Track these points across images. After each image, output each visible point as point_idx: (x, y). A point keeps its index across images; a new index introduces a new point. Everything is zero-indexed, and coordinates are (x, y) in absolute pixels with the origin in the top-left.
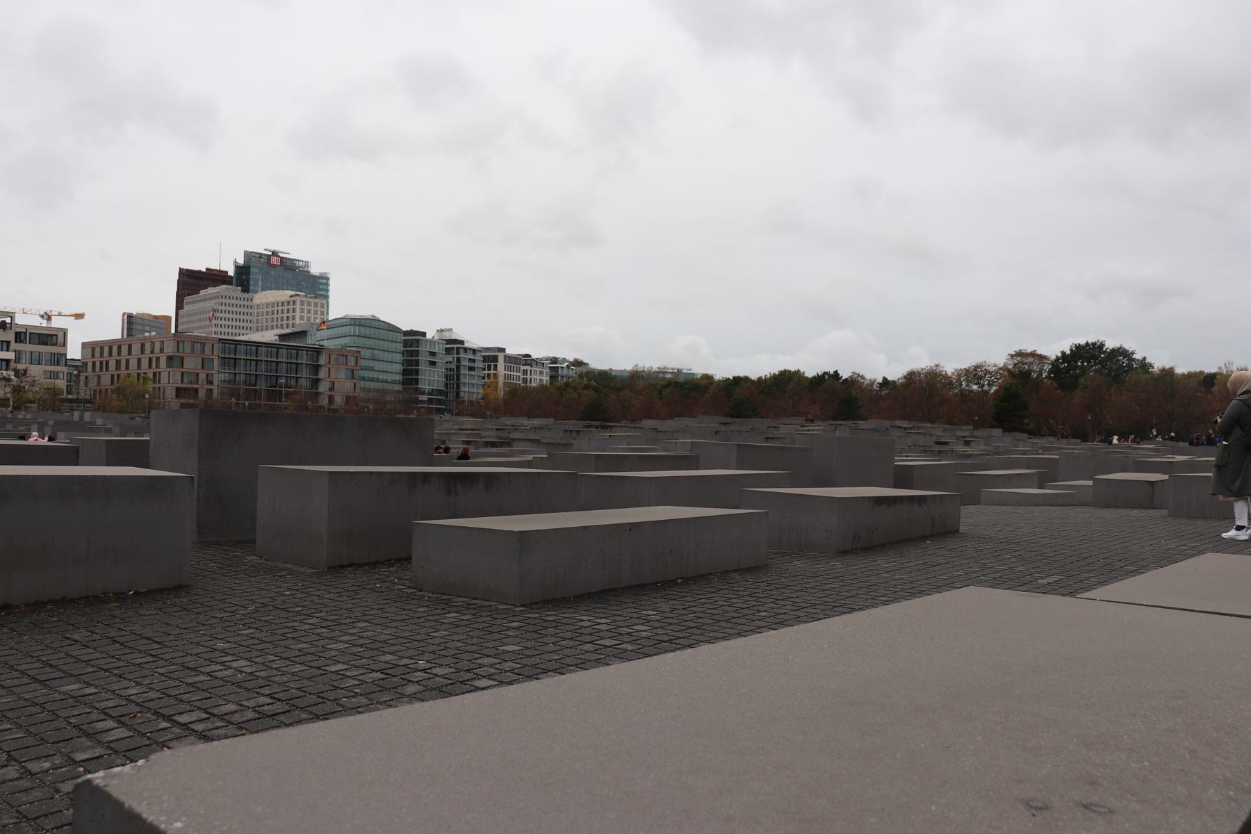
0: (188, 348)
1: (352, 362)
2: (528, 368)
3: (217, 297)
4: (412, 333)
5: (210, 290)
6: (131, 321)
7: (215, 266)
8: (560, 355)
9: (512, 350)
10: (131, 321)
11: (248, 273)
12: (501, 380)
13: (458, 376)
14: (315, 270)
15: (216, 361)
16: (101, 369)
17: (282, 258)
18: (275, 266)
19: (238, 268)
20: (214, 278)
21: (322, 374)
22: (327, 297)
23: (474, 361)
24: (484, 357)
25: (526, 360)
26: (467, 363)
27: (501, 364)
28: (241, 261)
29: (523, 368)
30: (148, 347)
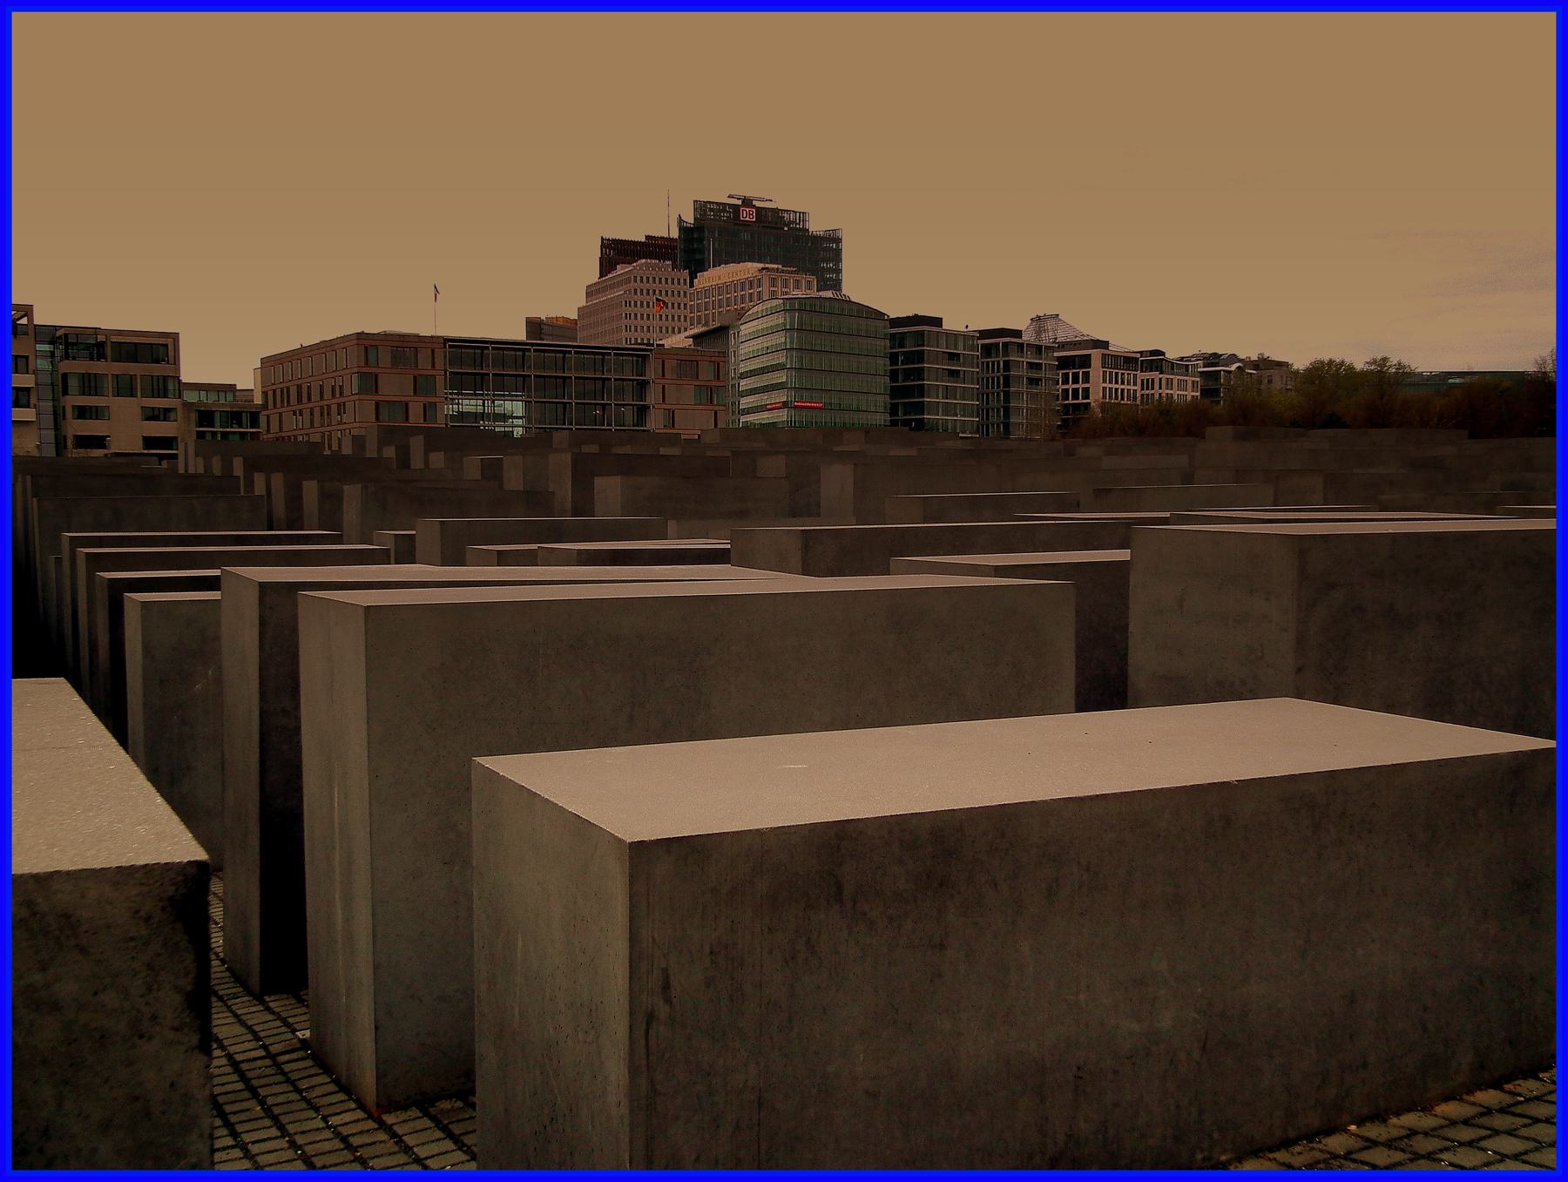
0: (385, 358)
1: (706, 373)
2: (1155, 375)
3: (628, 281)
4: (917, 320)
5: (621, 269)
6: (534, 326)
7: (661, 232)
8: (1223, 349)
10: (534, 326)
11: (701, 240)
12: (1095, 397)
14: (816, 226)
15: (440, 380)
16: (300, 401)
17: (758, 209)
18: (747, 224)
19: (683, 229)
20: (653, 248)
21: (652, 397)
22: (839, 271)
24: (1065, 363)
25: (1154, 361)
28: (689, 218)
29: (1141, 375)
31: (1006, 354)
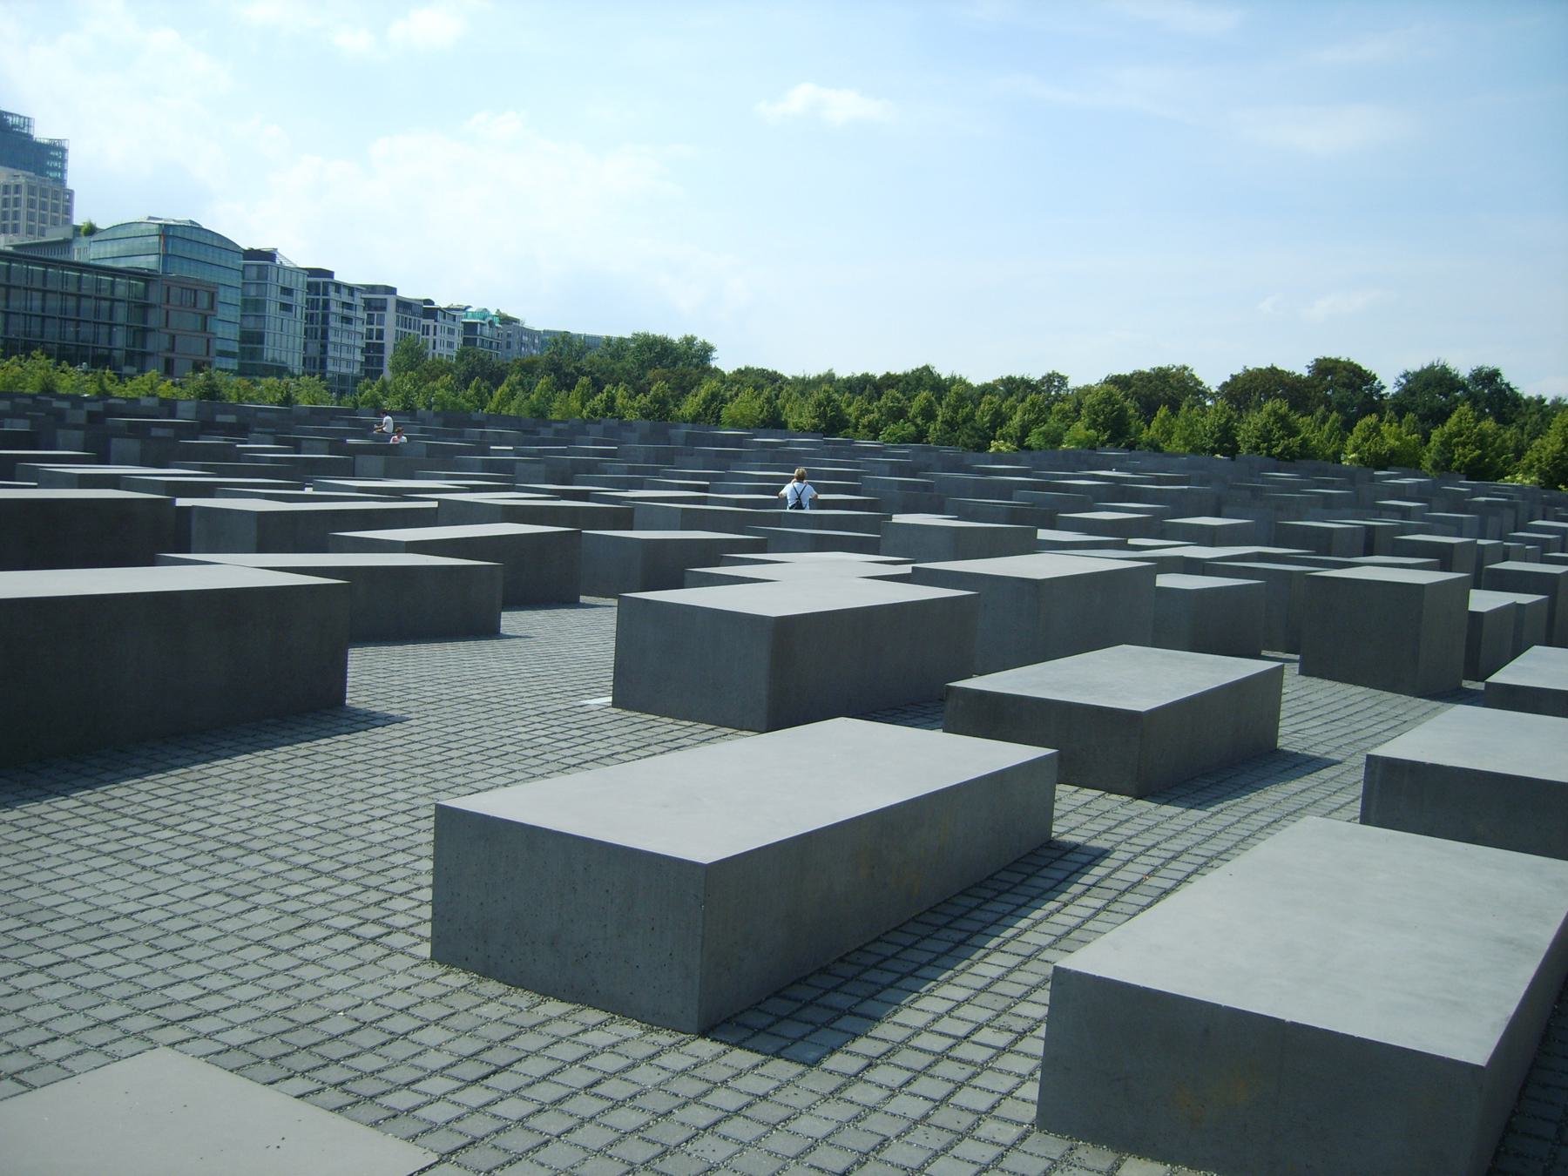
1: (204, 300)
2: (430, 322)
9: (405, 293)
14: (42, 133)
21: (154, 319)
23: (348, 306)
24: (369, 305)
25: (428, 310)
26: (339, 310)
27: (390, 315)
29: (425, 322)
31: (326, 293)
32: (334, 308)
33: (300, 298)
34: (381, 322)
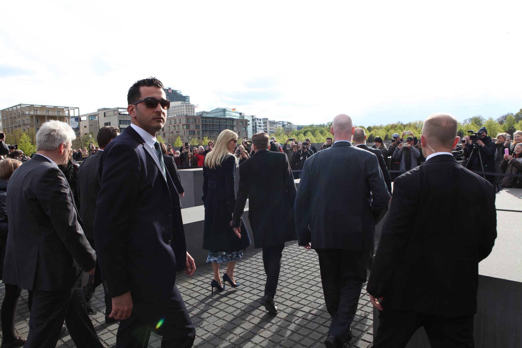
13: (256, 129)
23: (260, 123)
27: (268, 124)
30: (173, 121)
32: (257, 124)
33: (250, 123)
34: (266, 126)
